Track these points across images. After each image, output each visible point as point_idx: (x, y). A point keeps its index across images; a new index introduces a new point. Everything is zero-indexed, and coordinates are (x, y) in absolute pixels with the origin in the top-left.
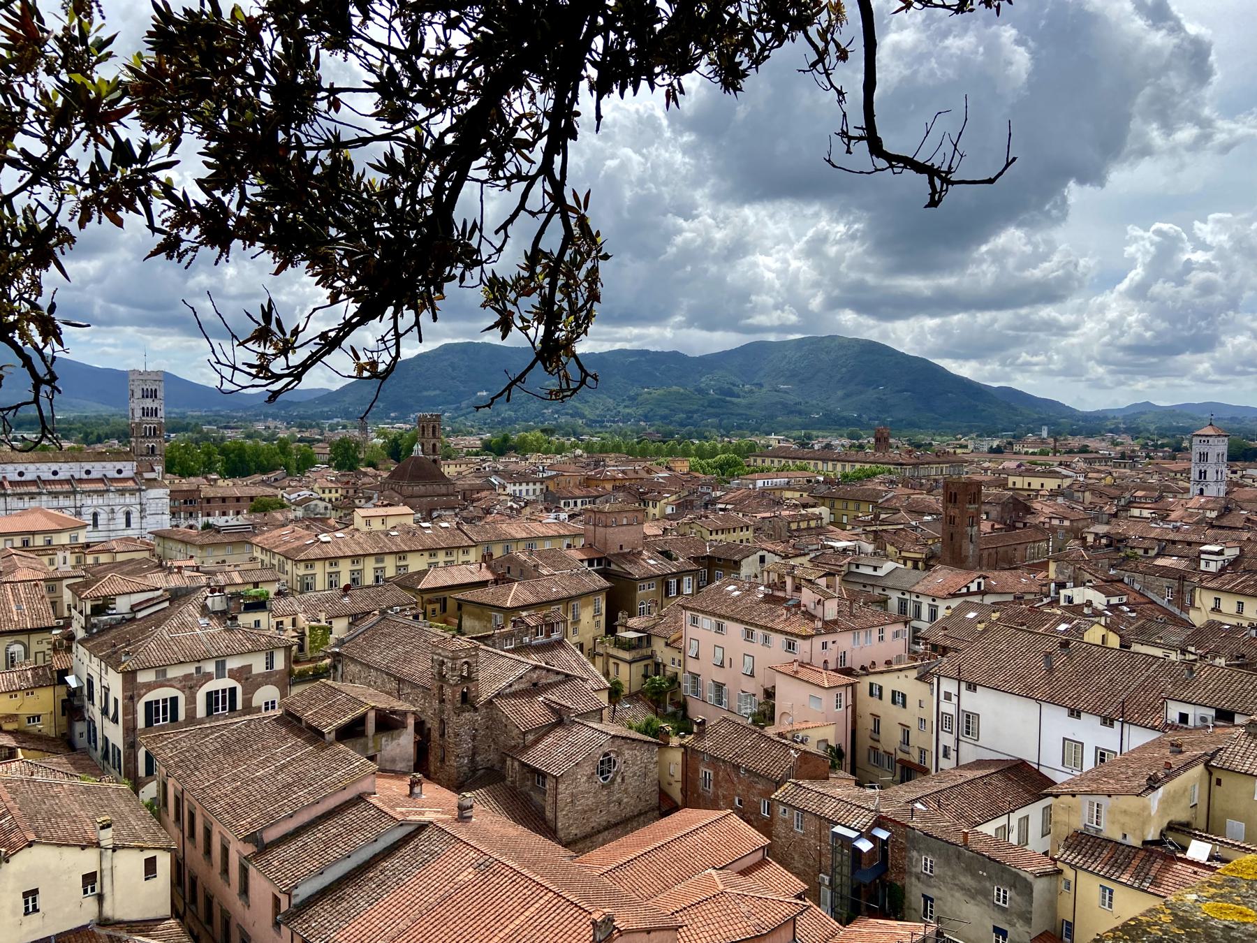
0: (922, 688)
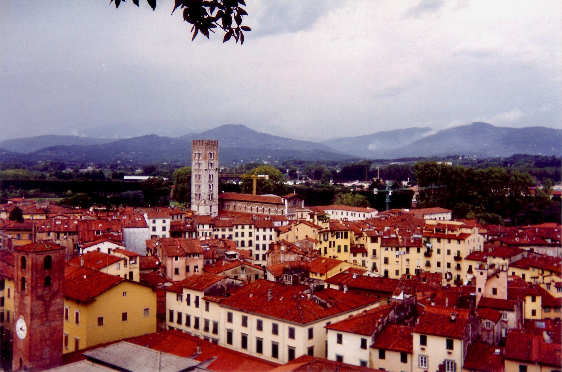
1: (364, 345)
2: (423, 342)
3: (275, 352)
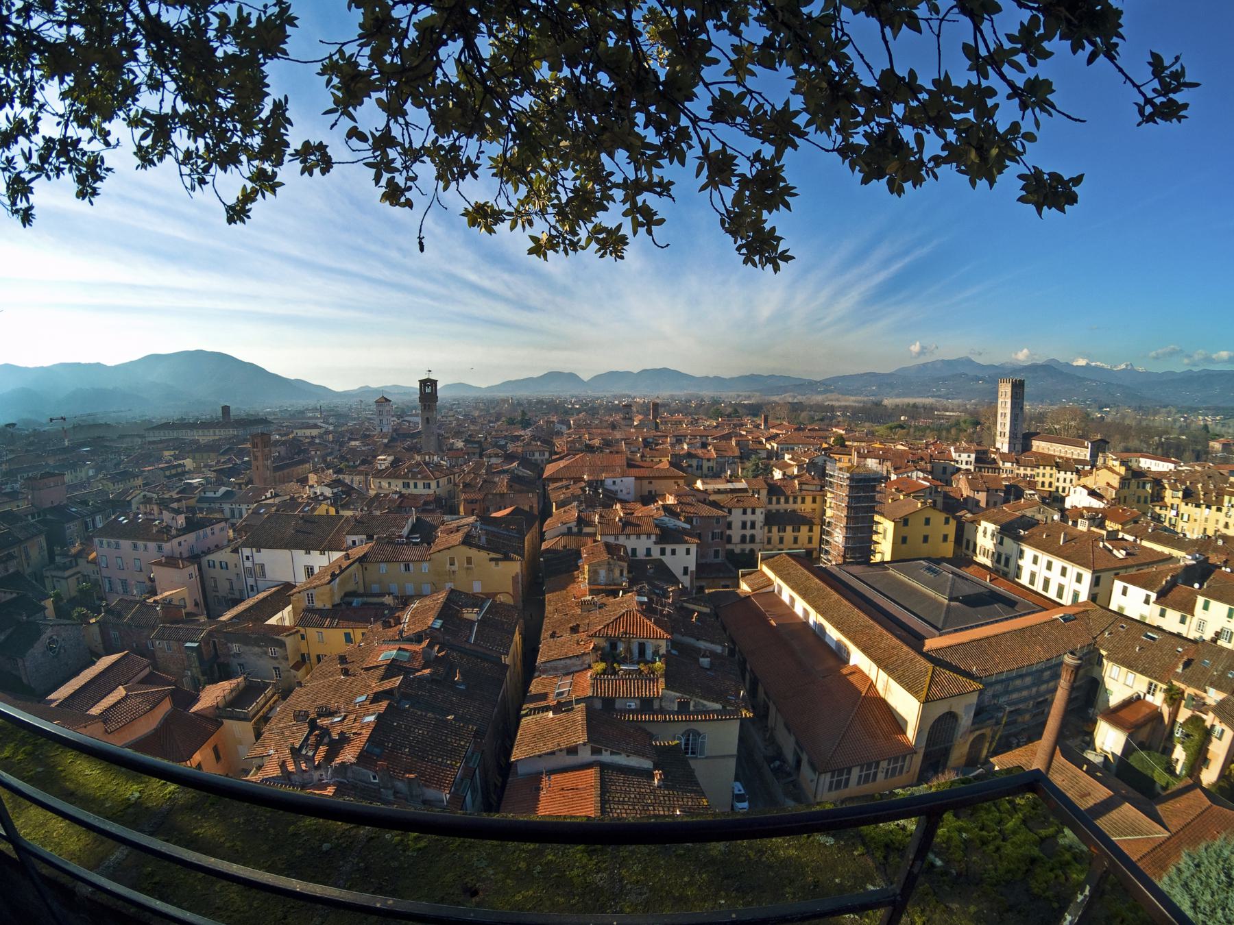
0: (234, 555)
3: (1060, 595)
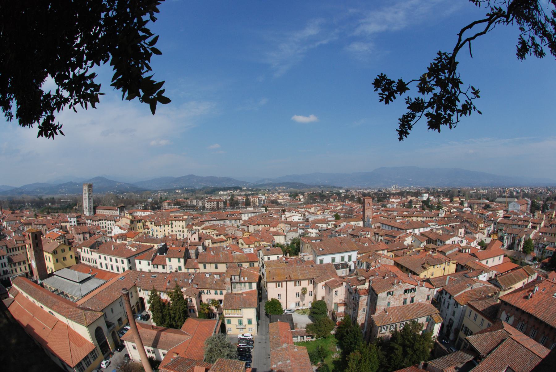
1: (149, 264)
2: (170, 261)
3: (118, 270)
